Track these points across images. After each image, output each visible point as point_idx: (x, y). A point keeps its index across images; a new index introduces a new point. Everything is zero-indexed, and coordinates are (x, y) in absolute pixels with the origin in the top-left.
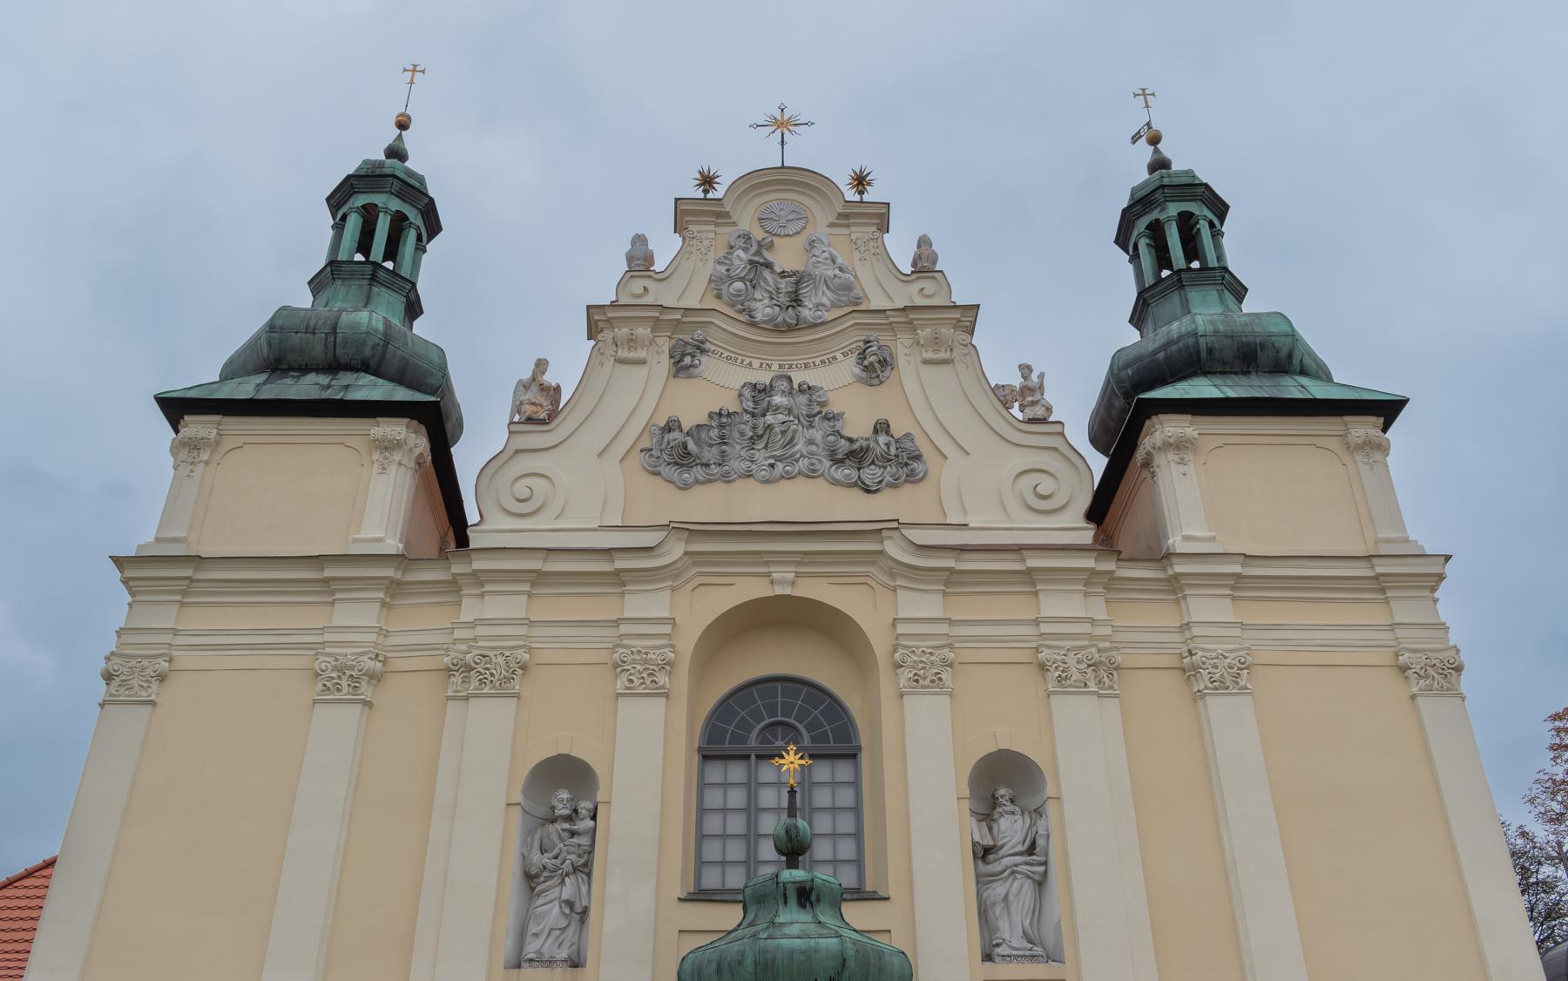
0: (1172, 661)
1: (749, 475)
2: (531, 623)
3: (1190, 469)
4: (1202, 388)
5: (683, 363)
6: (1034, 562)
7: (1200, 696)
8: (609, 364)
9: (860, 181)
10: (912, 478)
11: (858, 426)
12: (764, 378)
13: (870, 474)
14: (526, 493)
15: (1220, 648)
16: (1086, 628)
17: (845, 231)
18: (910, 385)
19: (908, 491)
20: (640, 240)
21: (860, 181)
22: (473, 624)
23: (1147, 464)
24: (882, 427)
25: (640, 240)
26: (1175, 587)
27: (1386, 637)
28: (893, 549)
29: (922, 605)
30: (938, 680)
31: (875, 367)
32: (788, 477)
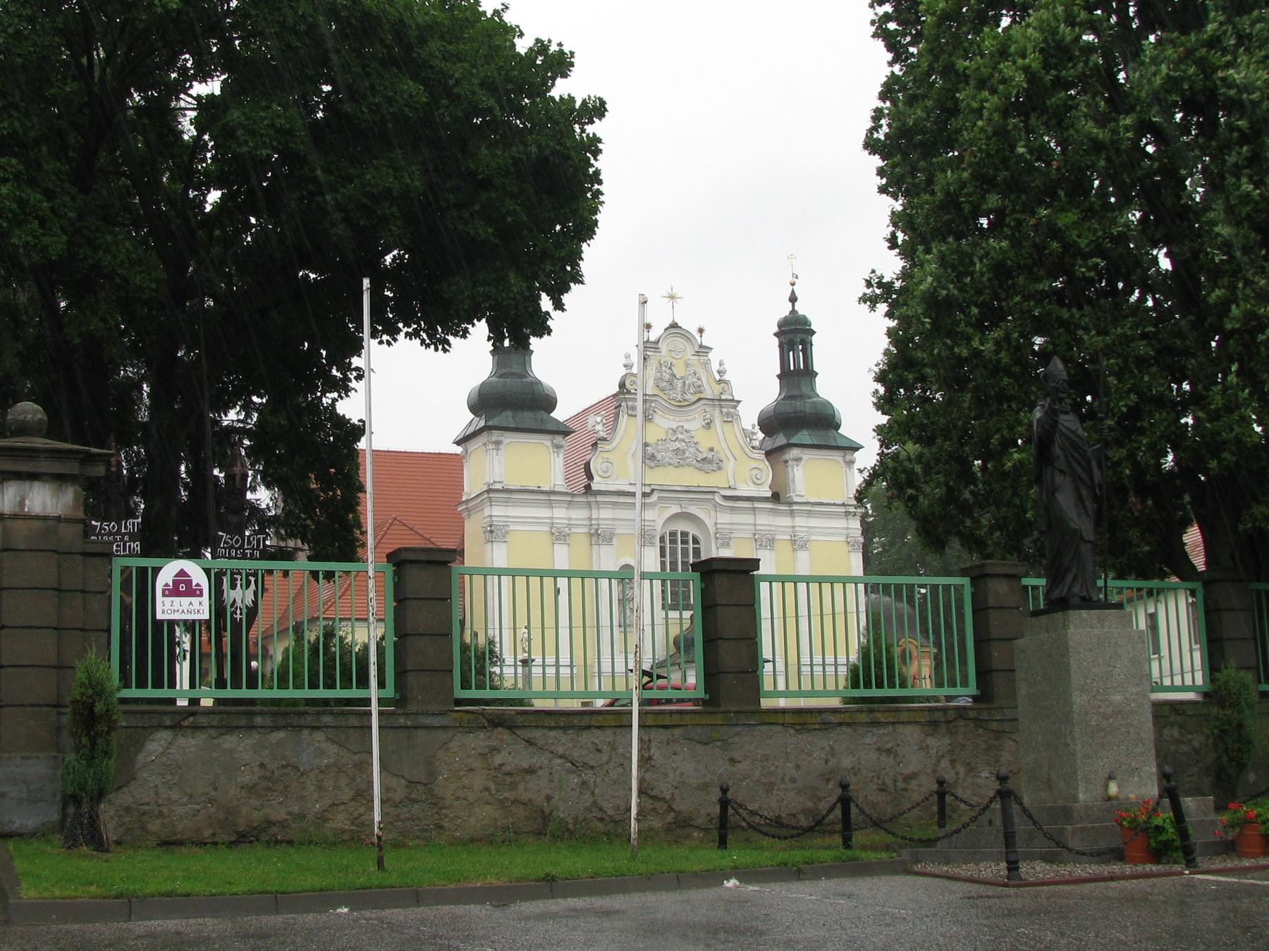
0: (789, 537)
1: (670, 464)
2: (615, 519)
3: (800, 468)
4: (804, 436)
5: (647, 418)
6: (757, 505)
7: (795, 550)
8: (626, 416)
9: (701, 331)
10: (720, 468)
11: (704, 447)
12: (674, 425)
13: (706, 466)
14: (604, 469)
15: (802, 534)
16: (768, 528)
17: (696, 358)
18: (719, 430)
19: (719, 473)
20: (628, 356)
21: (701, 331)
22: (598, 519)
23: (786, 462)
24: (712, 450)
25: (628, 356)
26: (792, 514)
27: (845, 532)
28: (718, 499)
29: (724, 518)
30: (728, 544)
31: (708, 425)
32: (682, 466)
